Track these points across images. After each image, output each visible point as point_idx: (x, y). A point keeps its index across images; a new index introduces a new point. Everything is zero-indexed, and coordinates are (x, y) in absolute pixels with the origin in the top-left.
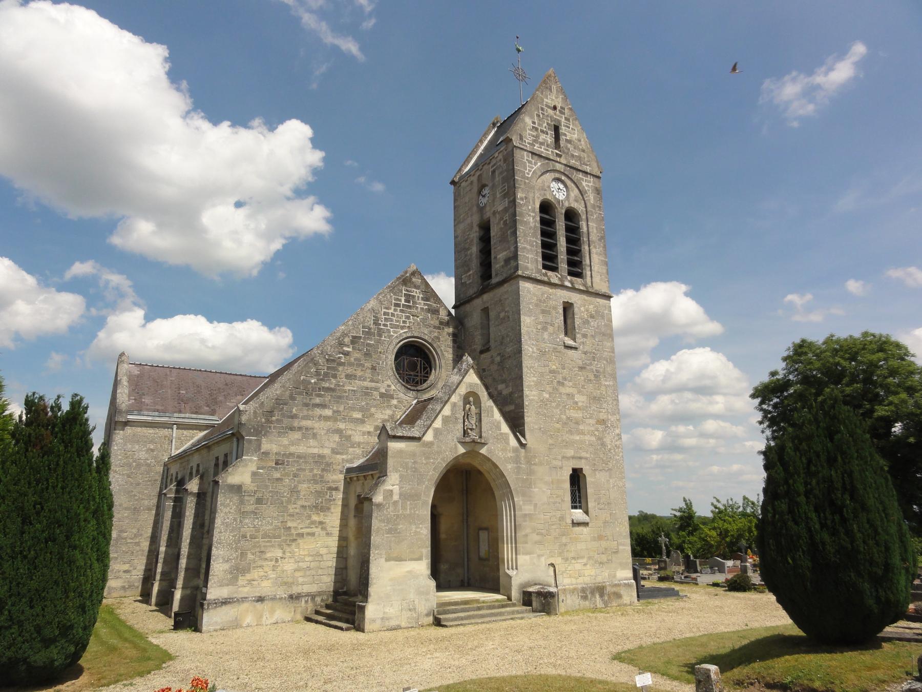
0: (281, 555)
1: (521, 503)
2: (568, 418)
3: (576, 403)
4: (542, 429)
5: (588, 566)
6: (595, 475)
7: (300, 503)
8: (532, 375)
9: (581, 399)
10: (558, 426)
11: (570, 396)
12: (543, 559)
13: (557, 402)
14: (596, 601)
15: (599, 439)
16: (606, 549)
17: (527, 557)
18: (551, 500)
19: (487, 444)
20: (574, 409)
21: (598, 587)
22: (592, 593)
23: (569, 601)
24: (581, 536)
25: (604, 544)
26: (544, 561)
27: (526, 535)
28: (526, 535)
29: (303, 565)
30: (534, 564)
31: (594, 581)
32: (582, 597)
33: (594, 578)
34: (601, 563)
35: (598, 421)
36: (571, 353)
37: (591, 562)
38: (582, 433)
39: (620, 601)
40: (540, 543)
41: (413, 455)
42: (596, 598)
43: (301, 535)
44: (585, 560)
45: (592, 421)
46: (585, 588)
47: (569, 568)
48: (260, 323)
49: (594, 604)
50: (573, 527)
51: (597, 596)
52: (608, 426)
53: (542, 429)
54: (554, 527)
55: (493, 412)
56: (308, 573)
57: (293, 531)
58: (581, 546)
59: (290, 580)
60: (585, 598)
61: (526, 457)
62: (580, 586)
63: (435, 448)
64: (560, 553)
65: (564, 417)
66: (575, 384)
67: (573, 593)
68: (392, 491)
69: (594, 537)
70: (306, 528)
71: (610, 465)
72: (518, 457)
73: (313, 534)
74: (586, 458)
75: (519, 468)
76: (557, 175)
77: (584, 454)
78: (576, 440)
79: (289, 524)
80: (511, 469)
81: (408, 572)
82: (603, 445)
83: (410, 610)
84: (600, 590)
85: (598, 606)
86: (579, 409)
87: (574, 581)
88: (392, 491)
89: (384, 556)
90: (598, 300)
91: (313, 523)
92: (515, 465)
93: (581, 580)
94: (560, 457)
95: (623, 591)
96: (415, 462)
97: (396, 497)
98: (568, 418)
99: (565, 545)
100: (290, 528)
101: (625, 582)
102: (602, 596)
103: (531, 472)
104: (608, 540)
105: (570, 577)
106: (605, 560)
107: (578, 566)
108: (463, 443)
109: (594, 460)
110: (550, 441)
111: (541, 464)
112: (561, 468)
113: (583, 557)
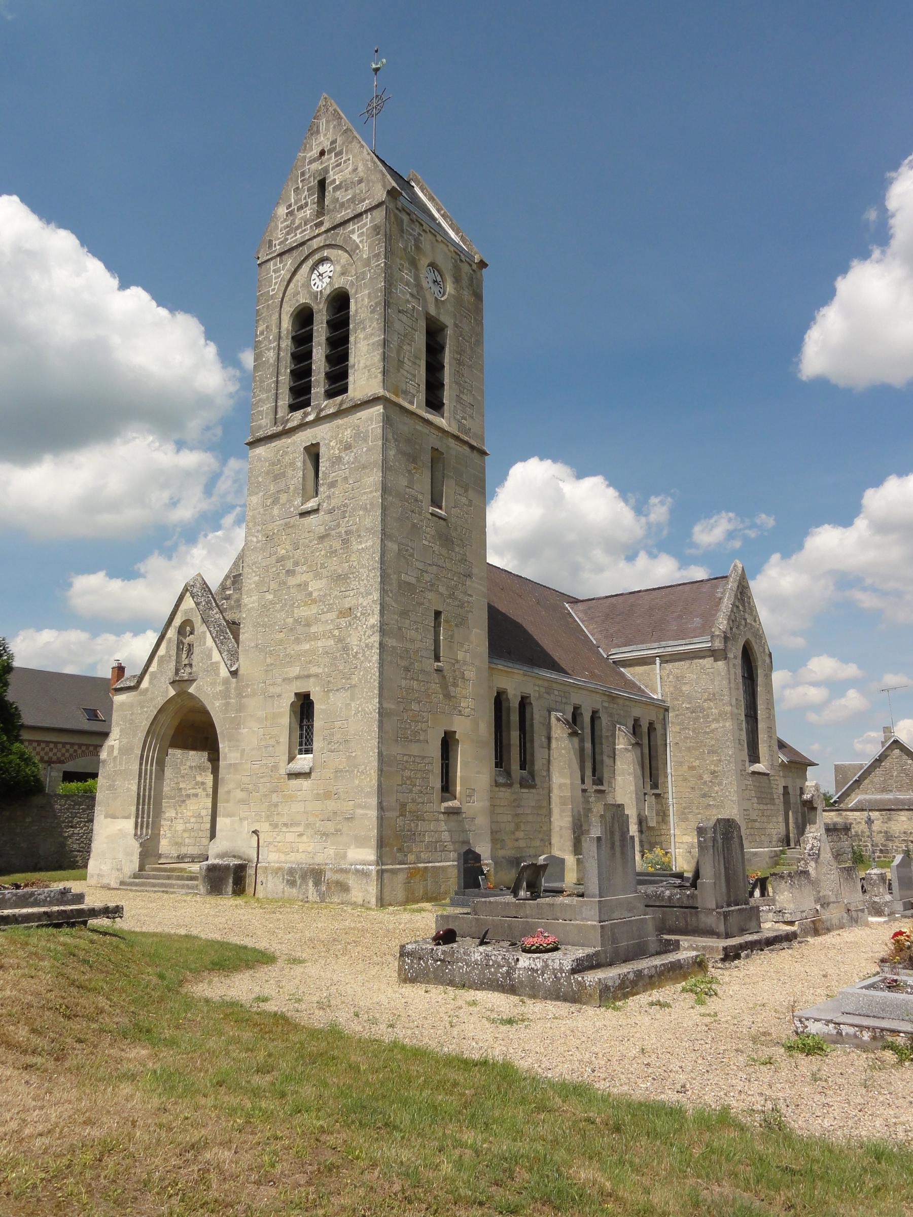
0: (174, 815)
1: (226, 750)
2: (296, 621)
3: (311, 594)
4: (259, 646)
5: (305, 837)
6: (329, 698)
7: (188, 764)
8: (254, 574)
9: (316, 586)
10: (282, 635)
11: (302, 586)
12: (245, 823)
13: (283, 601)
14: (307, 890)
15: (340, 640)
16: (335, 813)
17: (227, 821)
18: (263, 743)
19: (195, 680)
20: (306, 604)
21: (313, 869)
22: (304, 877)
23: (270, 885)
24: (299, 793)
25: (331, 805)
26: (247, 827)
27: (229, 792)
28: (229, 792)
29: (189, 826)
30: (235, 830)
31: (311, 861)
32: (288, 881)
33: (311, 855)
34: (324, 834)
35: (341, 612)
36: (312, 519)
37: (310, 832)
38: (316, 638)
39: (345, 897)
40: (242, 802)
41: (131, 706)
42: (307, 885)
43: (188, 796)
44: (300, 829)
45: (331, 616)
46: (294, 869)
47: (278, 838)
48: (617, 494)
49: (304, 893)
50: (289, 779)
51: (311, 884)
52: (356, 616)
53: (259, 646)
54: (262, 780)
55: (205, 638)
56: (192, 834)
57: (184, 793)
58: (297, 807)
59: (180, 840)
60: (292, 883)
61: (237, 688)
62: (287, 866)
63: (149, 695)
64: (268, 817)
65: (290, 620)
66: (310, 566)
67: (277, 873)
68: (113, 746)
69: (318, 794)
70: (192, 788)
71: (355, 680)
72: (227, 690)
73: (196, 795)
74: (316, 676)
75: (227, 704)
76: (310, 262)
77: (314, 670)
78: (306, 651)
79: (182, 786)
80: (218, 707)
81: (119, 830)
82: (346, 649)
83: (118, 870)
84: (316, 875)
85: (310, 898)
86: (314, 601)
87: (283, 857)
88: (113, 746)
89: (103, 813)
90: (359, 415)
91: (197, 783)
92: (224, 701)
93: (293, 857)
94: (279, 681)
95: (352, 881)
96: (132, 714)
97: (116, 753)
98: (296, 621)
99: (276, 805)
100: (181, 789)
101: (358, 867)
102: (317, 883)
103: (241, 708)
104: (338, 798)
105: (279, 851)
106: (332, 830)
107: (290, 837)
108: (173, 683)
109: (329, 675)
110: (269, 661)
111: (254, 694)
112: (279, 696)
113: (298, 824)
